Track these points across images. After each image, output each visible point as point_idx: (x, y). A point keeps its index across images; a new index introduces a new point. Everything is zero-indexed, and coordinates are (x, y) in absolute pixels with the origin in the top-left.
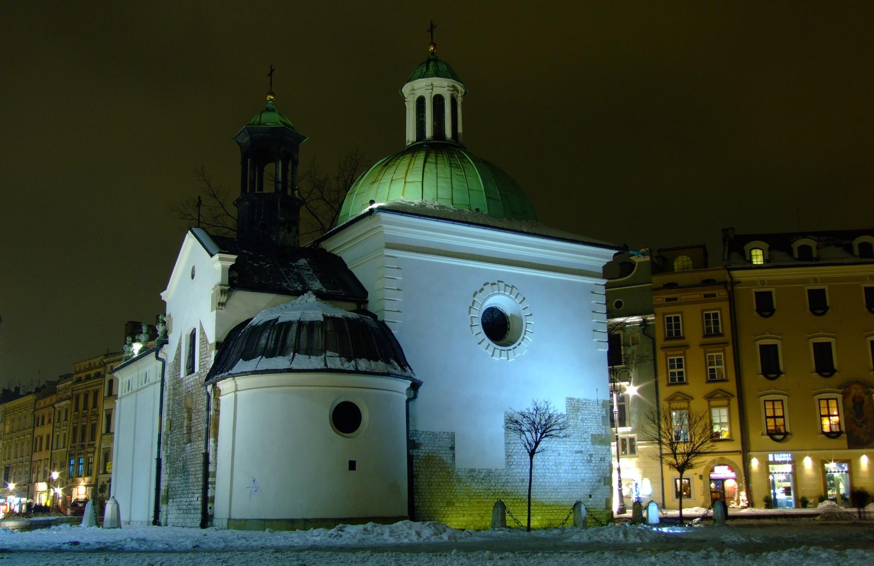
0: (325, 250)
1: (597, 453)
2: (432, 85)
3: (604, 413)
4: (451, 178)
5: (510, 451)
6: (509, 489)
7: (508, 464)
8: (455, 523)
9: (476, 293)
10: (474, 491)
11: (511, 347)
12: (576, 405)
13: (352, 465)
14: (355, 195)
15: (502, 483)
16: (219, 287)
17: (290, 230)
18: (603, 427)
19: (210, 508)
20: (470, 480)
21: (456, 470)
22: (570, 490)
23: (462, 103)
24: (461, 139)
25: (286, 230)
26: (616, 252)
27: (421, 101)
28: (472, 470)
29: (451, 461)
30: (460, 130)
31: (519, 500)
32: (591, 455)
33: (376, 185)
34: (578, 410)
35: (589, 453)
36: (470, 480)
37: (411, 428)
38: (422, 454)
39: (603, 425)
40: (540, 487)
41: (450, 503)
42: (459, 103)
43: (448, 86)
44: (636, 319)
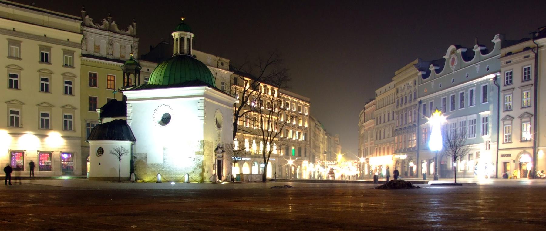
6: (164, 170)
7: (164, 162)
8: (147, 179)
28: (152, 164)
32: (195, 159)
37: (133, 152)
41: (145, 174)
44: (492, 76)
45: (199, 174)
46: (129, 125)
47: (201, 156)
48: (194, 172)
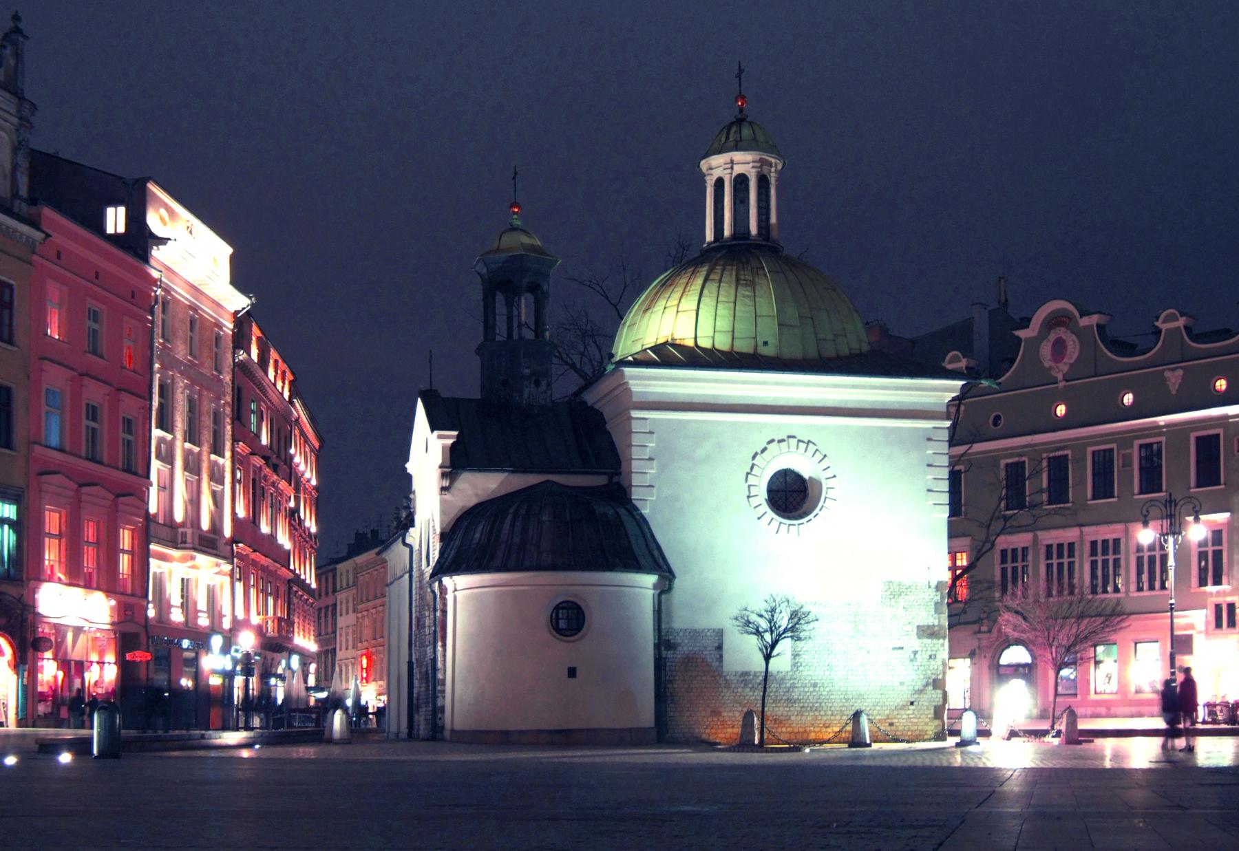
0: (585, 403)
1: (925, 649)
2: (732, 162)
3: (939, 597)
4: (735, 303)
5: (799, 649)
8: (723, 736)
9: (756, 454)
10: (747, 697)
11: (804, 520)
12: (896, 590)
13: (572, 672)
14: (626, 328)
15: (786, 687)
16: (439, 470)
17: (537, 384)
18: (936, 616)
19: (440, 719)
20: (742, 685)
21: (724, 674)
22: (883, 696)
23: (778, 180)
24: (774, 233)
25: (533, 386)
26: (964, 382)
27: (720, 183)
28: (746, 674)
29: (717, 663)
30: (773, 219)
31: (809, 709)
33: (648, 314)
34: (900, 595)
35: (914, 650)
36: (742, 685)
37: (663, 626)
38: (679, 656)
39: (936, 612)
40: (839, 693)
42: (773, 181)
43: (753, 162)
45: (932, 711)
46: (643, 512)
47: (941, 641)
48: (912, 703)
